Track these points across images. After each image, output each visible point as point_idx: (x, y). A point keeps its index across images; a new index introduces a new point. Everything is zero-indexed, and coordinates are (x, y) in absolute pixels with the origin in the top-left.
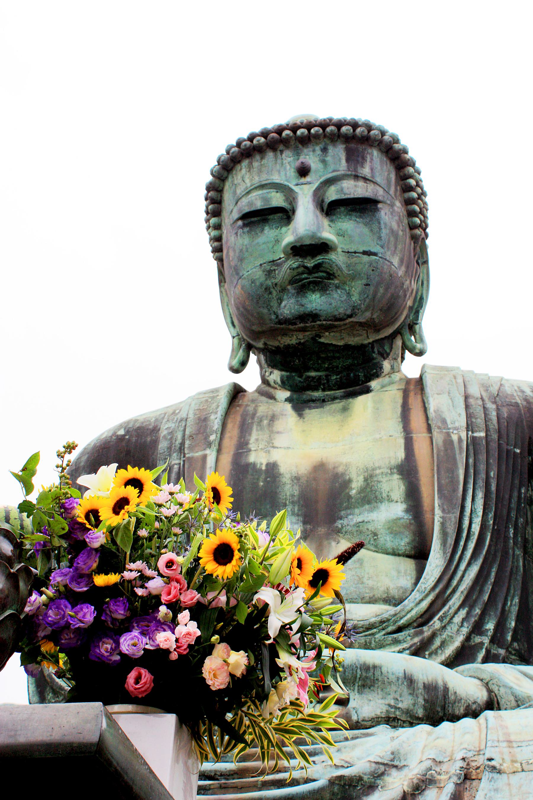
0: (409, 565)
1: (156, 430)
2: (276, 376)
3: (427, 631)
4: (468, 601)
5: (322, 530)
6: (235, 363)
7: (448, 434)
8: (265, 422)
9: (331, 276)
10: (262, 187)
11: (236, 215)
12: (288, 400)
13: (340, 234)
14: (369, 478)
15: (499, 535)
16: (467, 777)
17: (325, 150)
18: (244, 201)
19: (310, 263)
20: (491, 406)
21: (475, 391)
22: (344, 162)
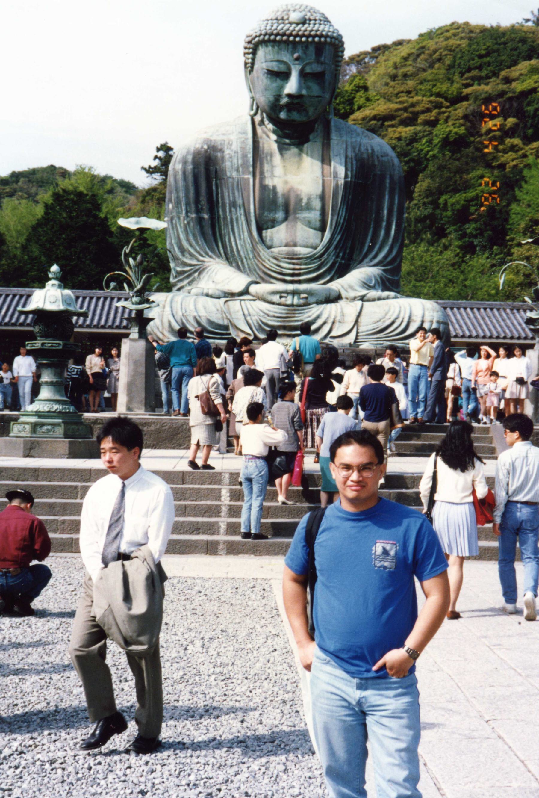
0: (319, 233)
1: (222, 151)
2: (271, 126)
3: (323, 259)
4: (336, 248)
5: (291, 217)
6: (252, 113)
7: (337, 181)
8: (269, 158)
9: (302, 106)
10: (278, 61)
11: (264, 65)
12: (276, 141)
13: (308, 88)
14: (309, 199)
15: (348, 221)
16: (333, 323)
17: (307, 47)
18: (270, 64)
19: (296, 101)
20: (354, 162)
21: (350, 154)
22: (314, 55)
